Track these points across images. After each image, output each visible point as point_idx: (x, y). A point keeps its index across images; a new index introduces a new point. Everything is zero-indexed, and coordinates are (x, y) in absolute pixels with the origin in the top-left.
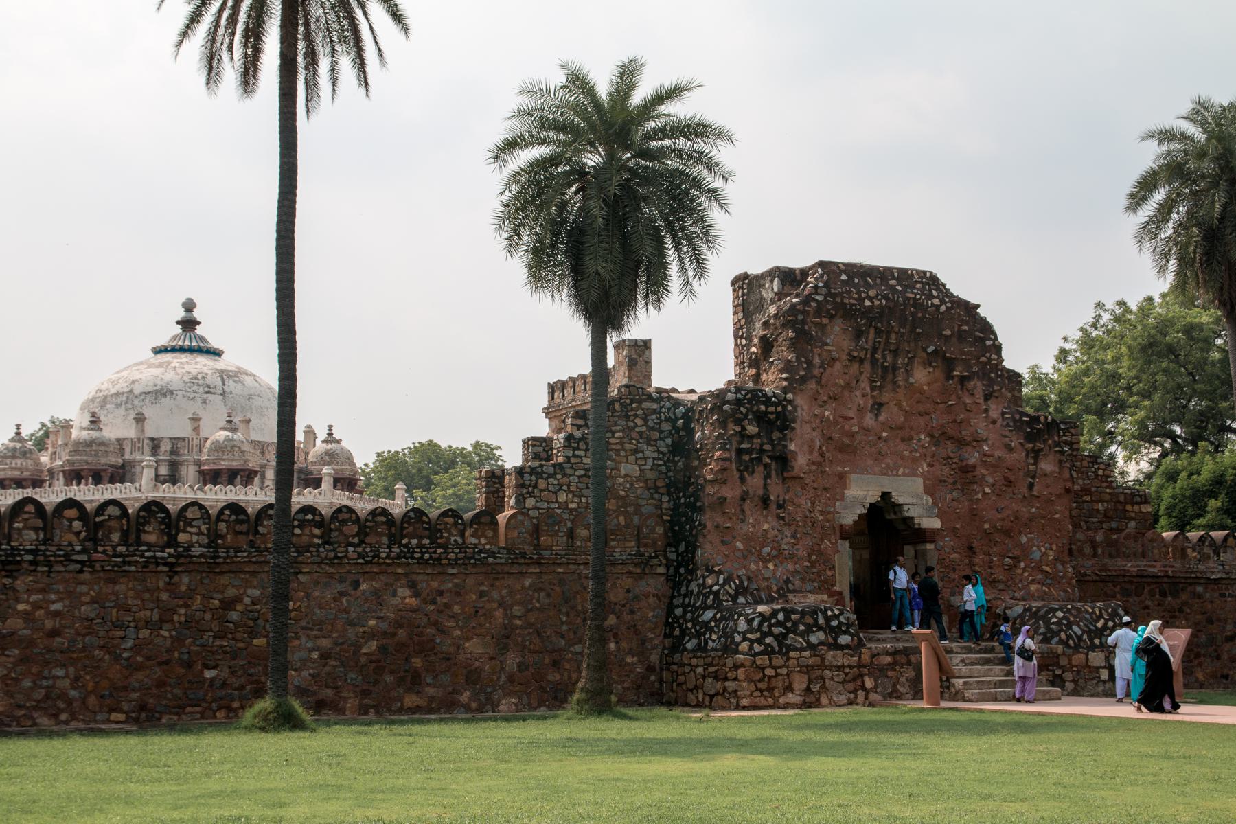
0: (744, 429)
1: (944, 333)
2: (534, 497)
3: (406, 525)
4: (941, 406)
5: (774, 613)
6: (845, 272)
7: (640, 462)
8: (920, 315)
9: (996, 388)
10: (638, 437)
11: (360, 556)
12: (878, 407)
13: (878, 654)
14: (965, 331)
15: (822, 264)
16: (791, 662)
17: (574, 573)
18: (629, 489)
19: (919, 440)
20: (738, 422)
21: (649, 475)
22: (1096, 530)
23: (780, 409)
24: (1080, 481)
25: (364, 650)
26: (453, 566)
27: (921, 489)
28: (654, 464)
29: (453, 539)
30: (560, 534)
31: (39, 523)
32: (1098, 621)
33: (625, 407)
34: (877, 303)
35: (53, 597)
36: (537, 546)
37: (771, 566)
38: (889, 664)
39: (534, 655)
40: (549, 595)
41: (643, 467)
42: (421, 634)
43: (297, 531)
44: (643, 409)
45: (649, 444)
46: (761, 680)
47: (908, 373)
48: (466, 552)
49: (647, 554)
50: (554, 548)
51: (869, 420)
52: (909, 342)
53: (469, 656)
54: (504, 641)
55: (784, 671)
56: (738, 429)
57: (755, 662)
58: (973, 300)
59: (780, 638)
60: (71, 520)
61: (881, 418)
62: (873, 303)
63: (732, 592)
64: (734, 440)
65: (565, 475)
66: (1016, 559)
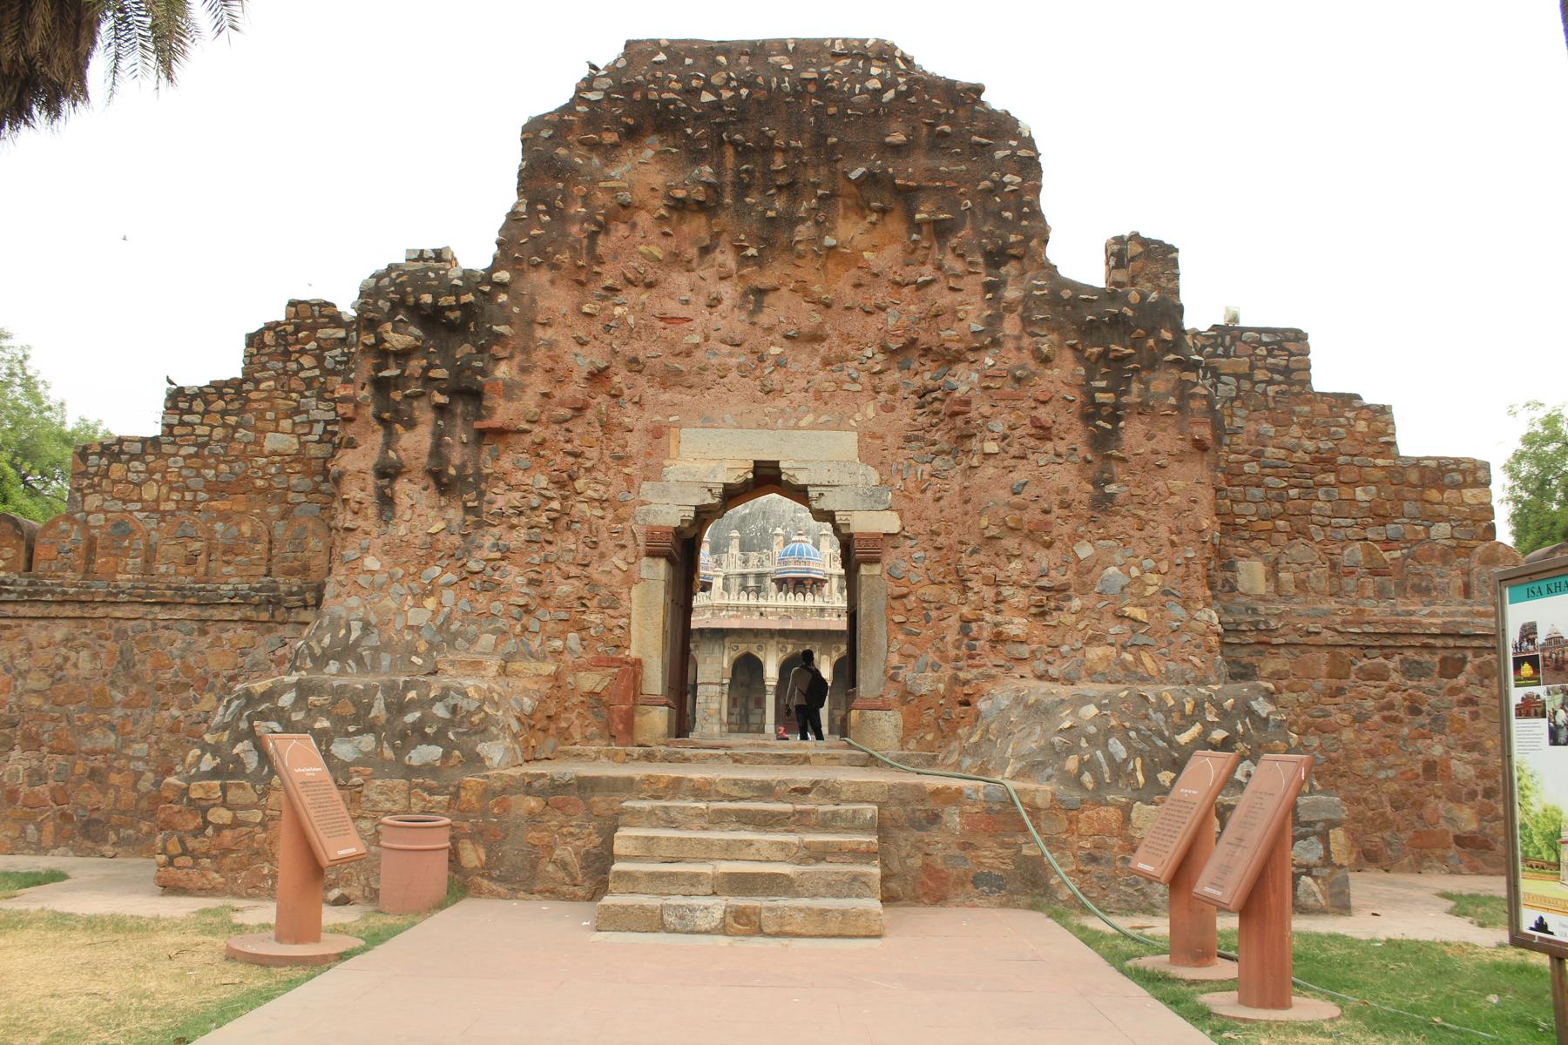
0: (380, 340)
1: (888, 139)
2: (102, 493)
4: (906, 290)
8: (832, 110)
10: (303, 387)
14: (943, 135)
21: (314, 451)
23: (468, 298)
24: (1309, 445)
28: (325, 430)
30: (132, 553)
32: (1189, 721)
33: (284, 338)
37: (430, 603)
40: (95, 656)
41: (304, 438)
44: (317, 340)
45: (320, 398)
46: (199, 832)
47: (822, 227)
49: (283, 588)
50: (118, 577)
55: (256, 816)
56: (370, 339)
57: (186, 791)
61: (764, 319)
63: (318, 651)
65: (161, 456)
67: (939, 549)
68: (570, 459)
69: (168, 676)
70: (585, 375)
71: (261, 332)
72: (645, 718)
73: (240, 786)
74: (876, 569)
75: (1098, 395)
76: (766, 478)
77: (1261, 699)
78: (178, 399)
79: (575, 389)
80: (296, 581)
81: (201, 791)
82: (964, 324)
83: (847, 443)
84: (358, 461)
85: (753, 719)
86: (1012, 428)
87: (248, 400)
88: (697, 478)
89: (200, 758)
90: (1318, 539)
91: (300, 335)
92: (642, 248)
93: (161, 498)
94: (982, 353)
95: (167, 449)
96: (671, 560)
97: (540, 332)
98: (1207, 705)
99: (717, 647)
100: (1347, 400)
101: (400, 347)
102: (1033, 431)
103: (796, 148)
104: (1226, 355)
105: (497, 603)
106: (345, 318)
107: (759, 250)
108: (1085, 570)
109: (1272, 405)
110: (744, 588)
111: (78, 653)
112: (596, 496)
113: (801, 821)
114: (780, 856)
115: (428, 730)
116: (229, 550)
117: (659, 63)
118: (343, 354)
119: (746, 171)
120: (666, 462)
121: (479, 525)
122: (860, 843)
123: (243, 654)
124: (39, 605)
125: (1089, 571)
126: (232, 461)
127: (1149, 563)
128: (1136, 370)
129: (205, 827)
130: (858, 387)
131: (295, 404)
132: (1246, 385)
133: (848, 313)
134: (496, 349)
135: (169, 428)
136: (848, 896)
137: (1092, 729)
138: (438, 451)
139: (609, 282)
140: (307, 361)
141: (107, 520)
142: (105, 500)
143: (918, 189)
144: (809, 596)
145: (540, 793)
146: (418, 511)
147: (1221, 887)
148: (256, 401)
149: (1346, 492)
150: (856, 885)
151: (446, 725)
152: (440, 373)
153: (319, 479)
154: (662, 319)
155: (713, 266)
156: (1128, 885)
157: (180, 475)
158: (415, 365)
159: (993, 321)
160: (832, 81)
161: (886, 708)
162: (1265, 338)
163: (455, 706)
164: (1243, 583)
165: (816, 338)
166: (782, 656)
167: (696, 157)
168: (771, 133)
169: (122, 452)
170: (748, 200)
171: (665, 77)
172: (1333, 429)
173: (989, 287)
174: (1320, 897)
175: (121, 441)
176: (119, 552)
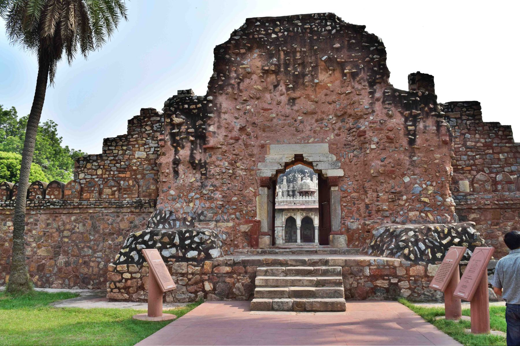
0: (172, 120)
1: (334, 46)
2: (84, 173)
3: (15, 190)
4: (342, 96)
7: (147, 150)
8: (315, 38)
9: (378, 76)
10: (147, 137)
12: (292, 101)
13: (219, 265)
16: (143, 269)
17: (99, 212)
18: (139, 165)
21: (152, 157)
22: (497, 173)
24: (483, 140)
26: (33, 210)
27: (327, 149)
28: (155, 150)
29: (37, 196)
30: (95, 192)
32: (445, 237)
34: (280, 34)
36: (81, 199)
37: (191, 205)
38: (227, 273)
39: (74, 257)
40: (84, 225)
41: (148, 153)
45: (153, 140)
46: (120, 281)
48: (41, 203)
49: (143, 201)
50: (90, 200)
51: (287, 110)
52: (311, 57)
53: (39, 257)
54: (58, 249)
55: (138, 275)
56: (169, 120)
57: (116, 268)
58: (359, 23)
61: (296, 108)
62: (277, 35)
63: (156, 221)
64: (169, 127)
65: (103, 160)
66: (399, 194)
67: (358, 181)
68: (234, 156)
69: (107, 231)
70: (238, 129)
71: (133, 119)
72: (262, 240)
73: (134, 266)
74: (336, 188)
75: (409, 127)
76: (299, 159)
77: (471, 228)
78: (107, 141)
79: (236, 133)
80: (146, 199)
81: (120, 268)
82: (362, 106)
84: (167, 159)
85: (293, 238)
86: (380, 140)
87: (130, 141)
88: (276, 161)
89: (120, 258)
90: (487, 172)
91: (145, 120)
92: (255, 87)
93: (103, 173)
94: (369, 115)
95: (105, 158)
96: (269, 188)
97: (223, 116)
98: (452, 230)
99: (280, 215)
100: (496, 125)
101: (178, 122)
102: (388, 140)
103: (304, 51)
104: (452, 111)
105: (213, 204)
106: (160, 113)
107: (293, 85)
108: (407, 186)
109: (469, 127)
110: (289, 195)
111: (79, 224)
112: (243, 168)
114: (310, 284)
115: (193, 246)
116: (125, 190)
117: (258, 25)
118: (159, 125)
119: (288, 59)
120: (266, 156)
121: (206, 178)
122: (336, 280)
123: (131, 223)
124: (66, 209)
125: (408, 186)
126: (125, 161)
127: (429, 183)
128: (423, 119)
129: (122, 279)
130: (328, 129)
131: (144, 142)
132: (459, 121)
133: (323, 104)
134: (209, 122)
135: (104, 151)
136: (334, 297)
137: (413, 240)
138: (192, 156)
139: (245, 98)
140: (148, 128)
141: (86, 181)
142: (85, 175)
143: (345, 62)
144: (310, 197)
145: (229, 265)
146: (186, 175)
147: (464, 293)
148: (132, 141)
149: (496, 156)
150: (336, 294)
151: (199, 244)
152: (191, 130)
153: (153, 166)
154: (262, 109)
155: (278, 91)
156: (428, 292)
157: (109, 166)
158: (183, 128)
159: (371, 104)
160: (315, 28)
161: (341, 234)
162: (465, 105)
163: (201, 238)
164: (461, 189)
165: (313, 113)
166: (302, 217)
167: (271, 56)
168: (295, 46)
169: (90, 159)
170: (289, 69)
171: (260, 30)
172: (491, 134)
173: (370, 93)
174: (495, 295)
175: (90, 156)
176: (90, 191)
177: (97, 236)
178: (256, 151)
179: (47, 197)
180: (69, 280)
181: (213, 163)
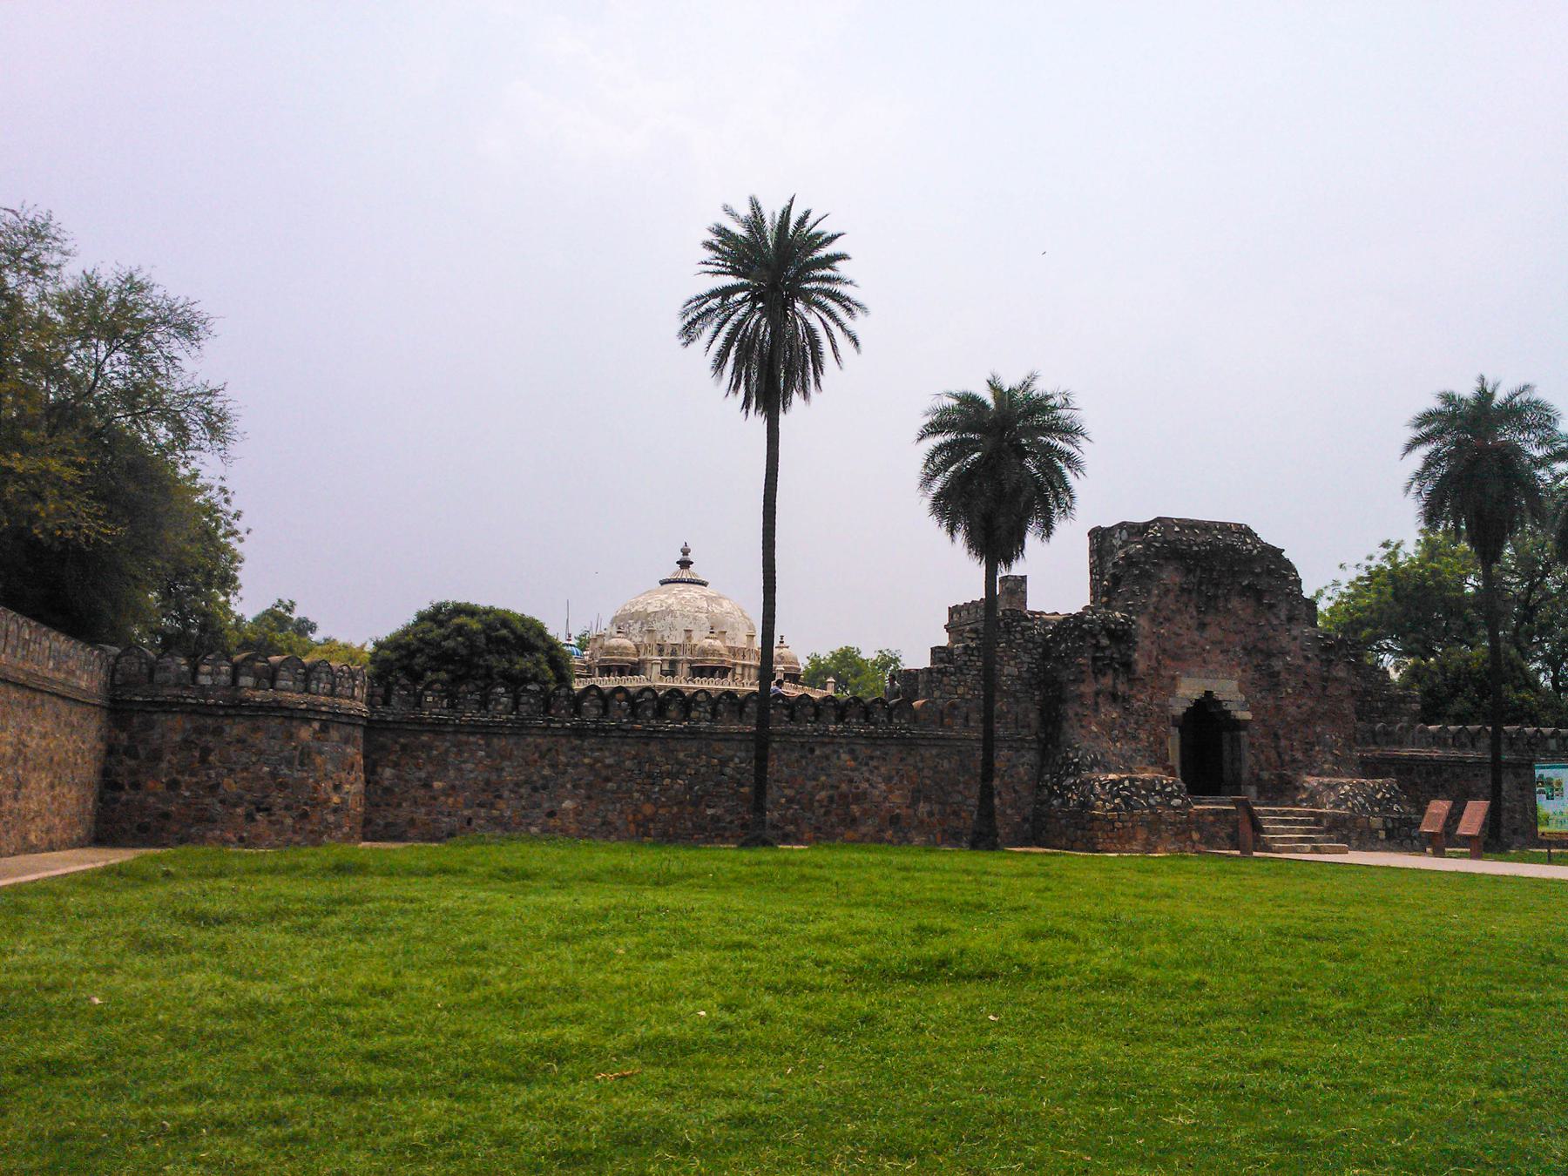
0: (1098, 642)
5: (1121, 781)
6: (1177, 525)
11: (815, 730)
12: (1202, 626)
15: (1159, 519)
19: (1235, 652)
20: (1094, 636)
21: (1025, 675)
25: (817, 798)
31: (599, 702)
35: (607, 754)
37: (1118, 744)
40: (950, 762)
42: (857, 788)
43: (772, 711)
45: (1025, 653)
47: (1227, 600)
56: (1094, 642)
59: (1126, 800)
60: (620, 701)
61: (1205, 635)
83: (1235, 683)
113: (1302, 823)
138: (1114, 686)
158: (1108, 653)
161: (1251, 784)
169: (946, 672)
177: (966, 777)
178: (1166, 681)
179: (895, 721)
180: (935, 835)
181: (1134, 696)
